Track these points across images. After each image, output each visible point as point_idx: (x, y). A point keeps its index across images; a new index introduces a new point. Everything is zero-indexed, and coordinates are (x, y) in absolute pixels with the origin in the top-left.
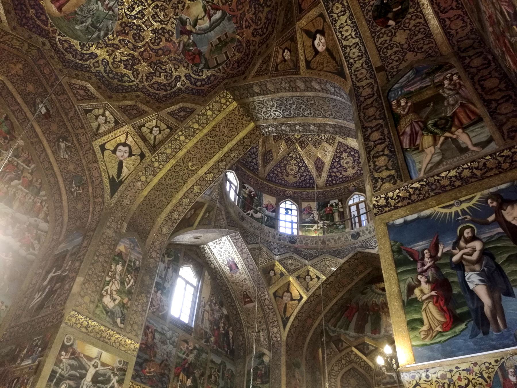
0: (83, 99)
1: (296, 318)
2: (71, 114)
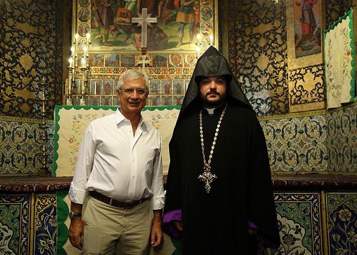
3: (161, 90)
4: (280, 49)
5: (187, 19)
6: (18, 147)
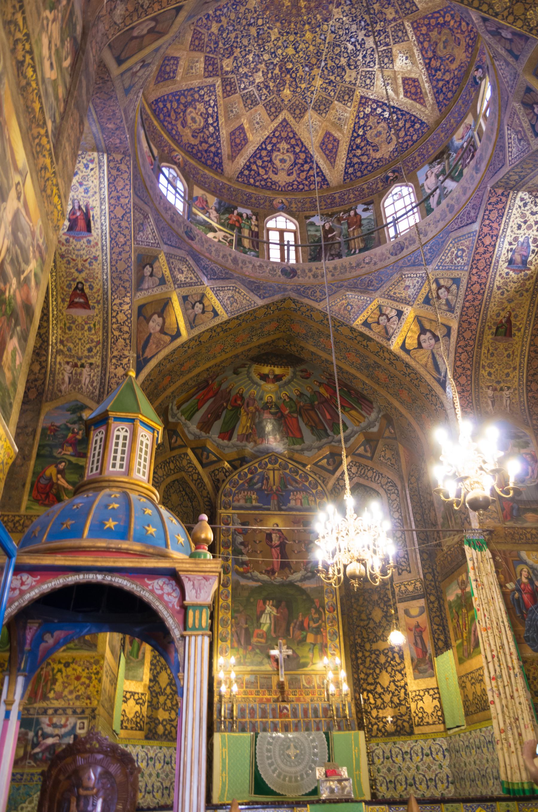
1: (159, 364)
3: (300, 713)
4: (399, 668)
5: (316, 640)
6: (158, 775)
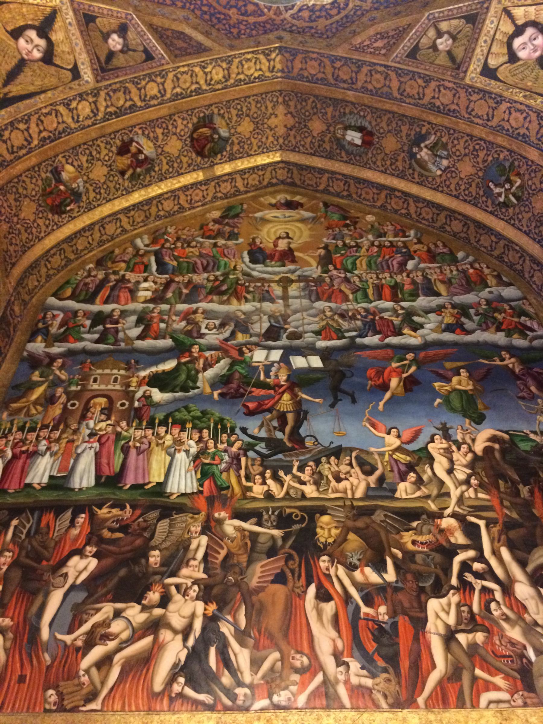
0: (390, 48)
2: (395, 84)
